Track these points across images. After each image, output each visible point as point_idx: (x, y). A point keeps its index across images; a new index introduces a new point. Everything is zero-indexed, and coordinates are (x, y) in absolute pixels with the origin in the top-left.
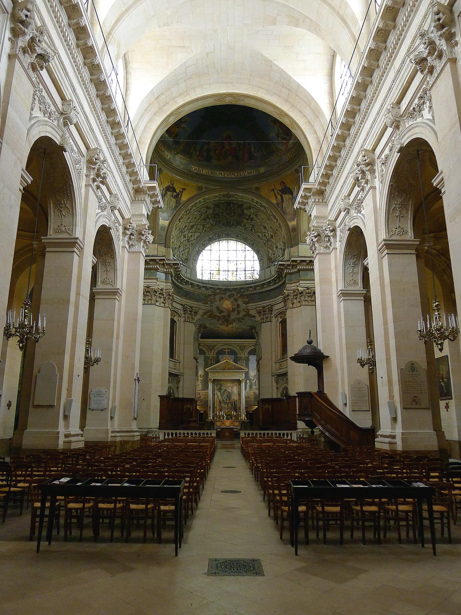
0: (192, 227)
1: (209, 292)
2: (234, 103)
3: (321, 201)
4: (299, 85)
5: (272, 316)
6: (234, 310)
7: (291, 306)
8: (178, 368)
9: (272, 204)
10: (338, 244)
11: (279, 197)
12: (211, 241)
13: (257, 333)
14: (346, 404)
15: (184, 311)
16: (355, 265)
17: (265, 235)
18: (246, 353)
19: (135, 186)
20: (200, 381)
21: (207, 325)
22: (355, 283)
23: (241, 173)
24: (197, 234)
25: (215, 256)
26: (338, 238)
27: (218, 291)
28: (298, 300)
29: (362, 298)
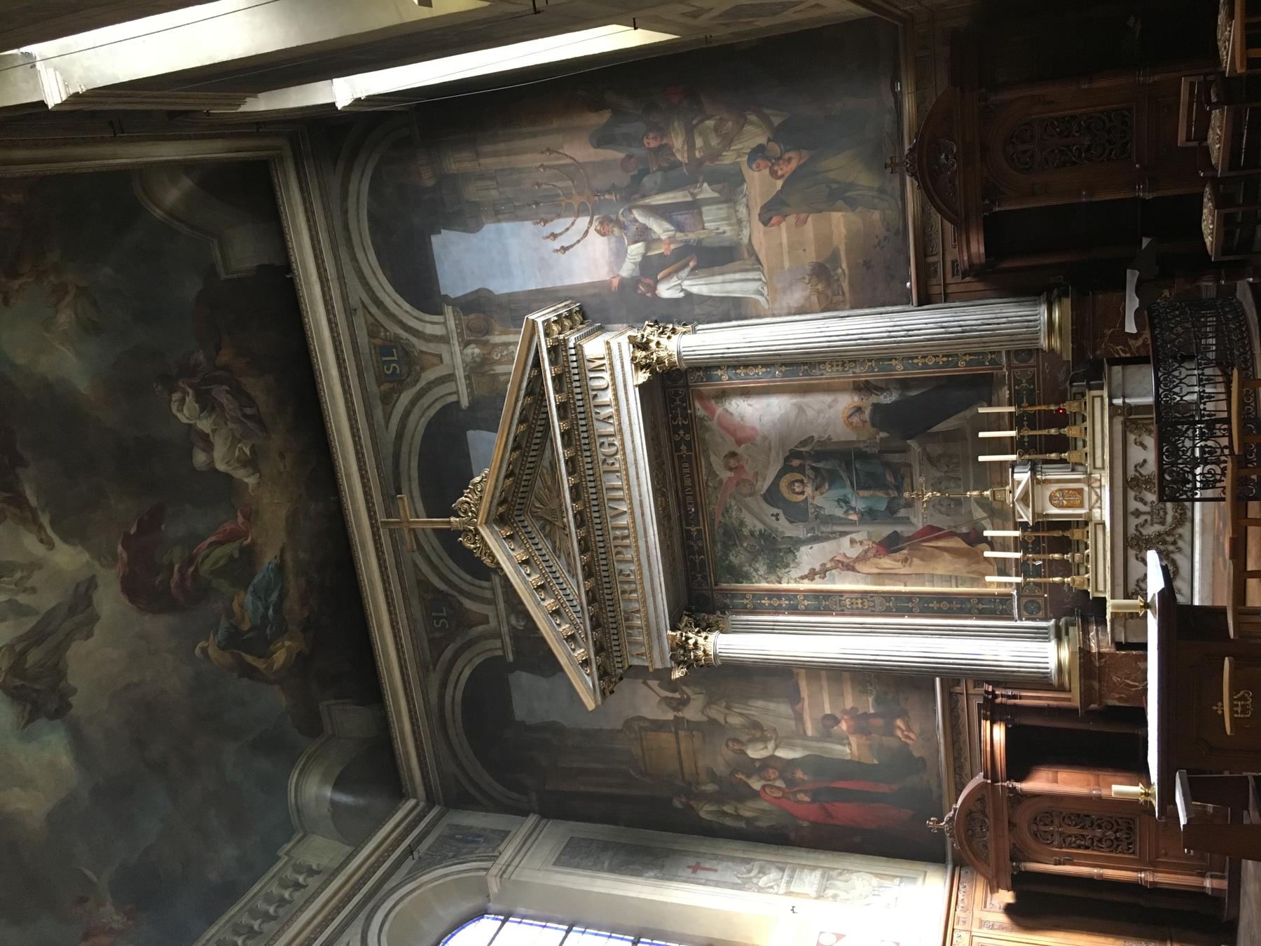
18: (431, 326)
20: (716, 713)
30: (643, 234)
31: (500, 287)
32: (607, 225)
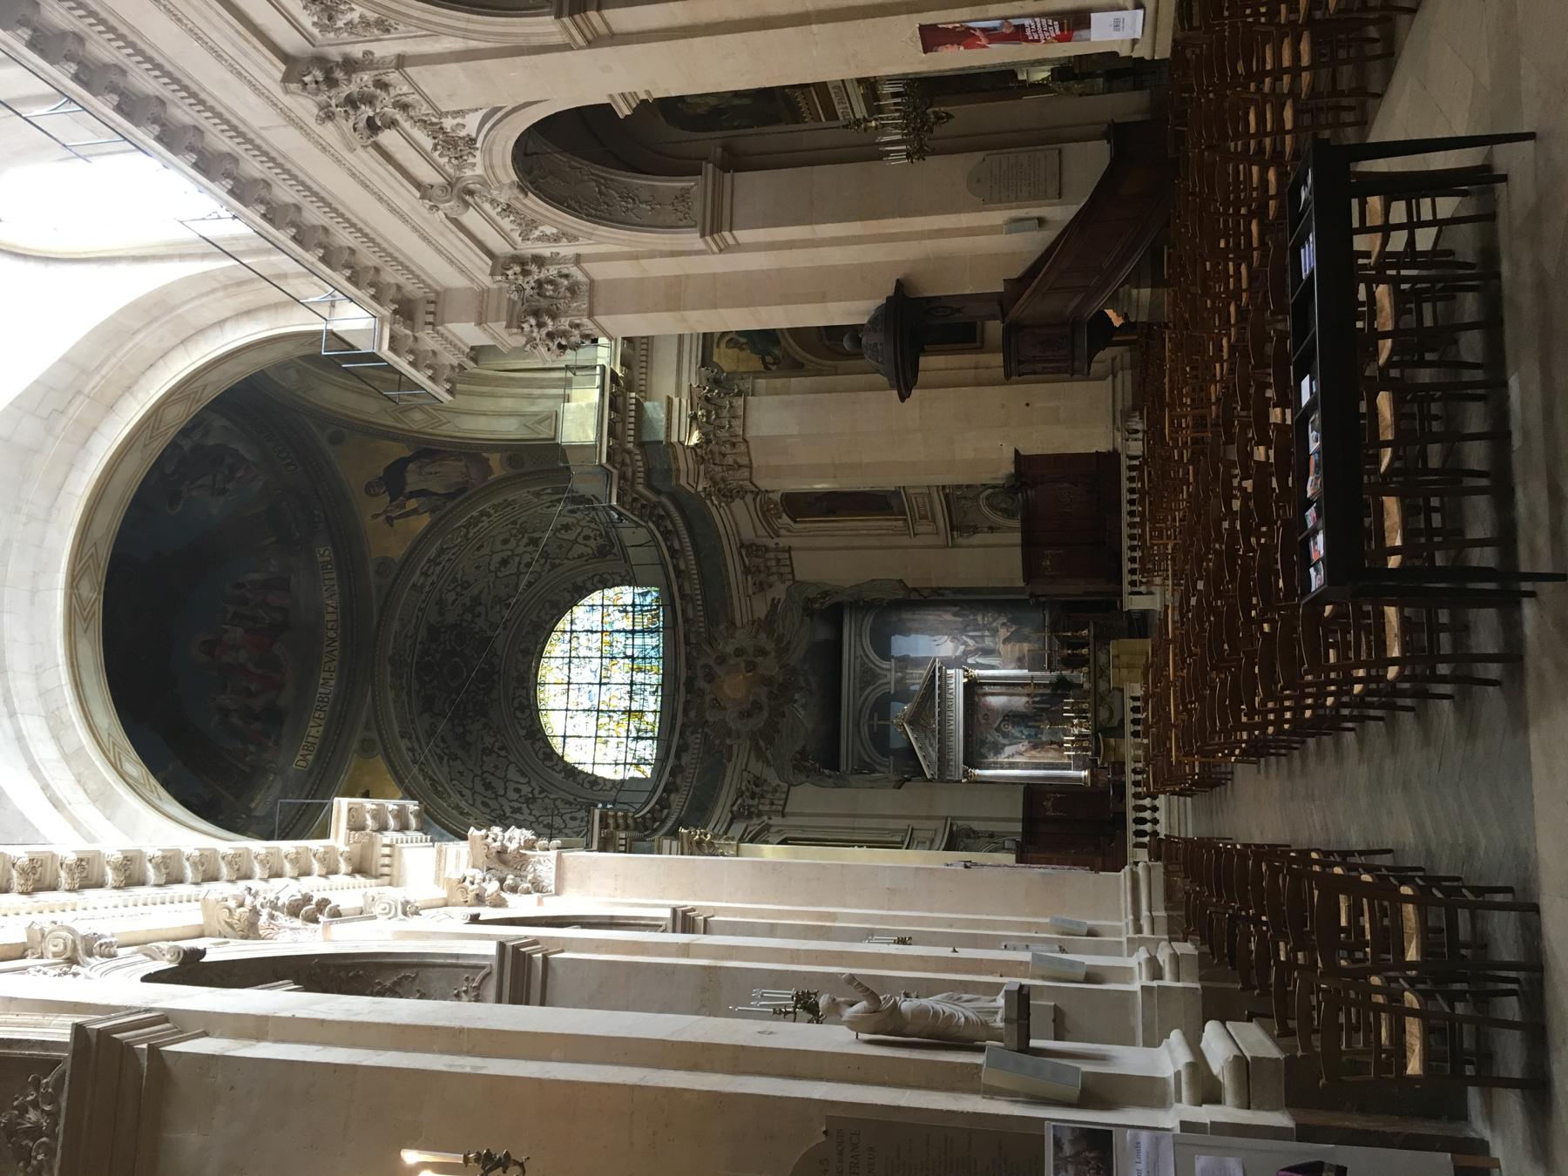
0: (488, 786)
1: (695, 740)
2: (101, 577)
3: (431, 308)
4: (64, 359)
5: (771, 543)
6: (751, 666)
7: (745, 473)
8: (930, 834)
9: (431, 527)
10: (566, 250)
11: (412, 504)
12: (537, 734)
13: (825, 594)
14: (1041, 222)
15: (750, 816)
16: (628, 195)
17: (528, 565)
18: (885, 665)
19: (344, 867)
21: (797, 748)
22: (683, 196)
23: (328, 617)
24: (513, 774)
25: (584, 724)
26: (545, 250)
27: (692, 714)
28: (727, 449)
29: (728, 176)
30: (965, 643)
31: (912, 655)
32: (954, 639)
